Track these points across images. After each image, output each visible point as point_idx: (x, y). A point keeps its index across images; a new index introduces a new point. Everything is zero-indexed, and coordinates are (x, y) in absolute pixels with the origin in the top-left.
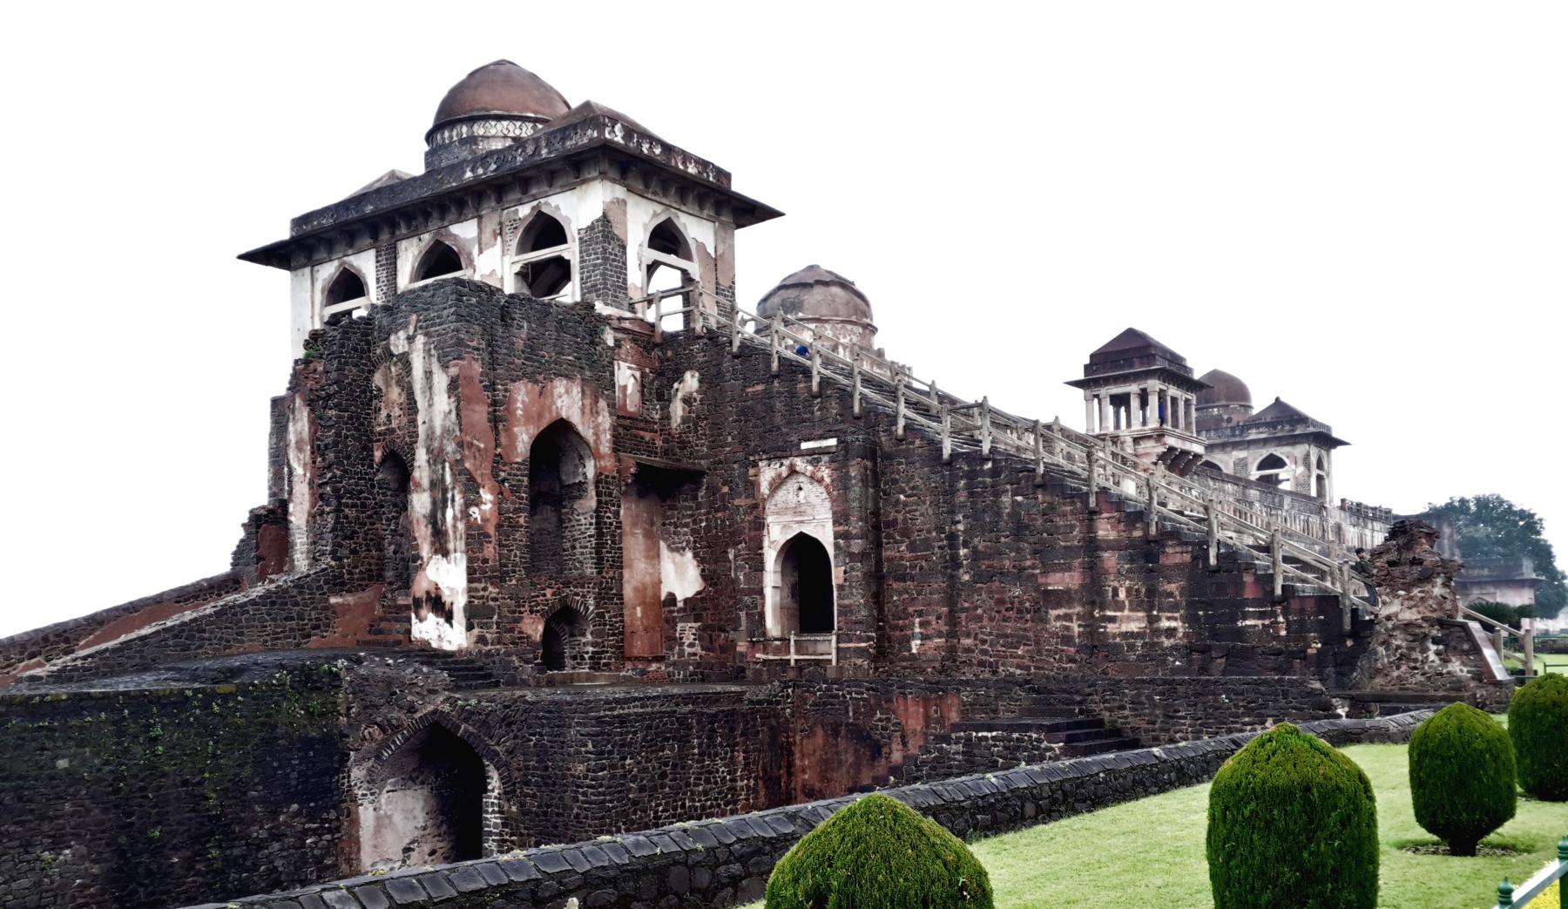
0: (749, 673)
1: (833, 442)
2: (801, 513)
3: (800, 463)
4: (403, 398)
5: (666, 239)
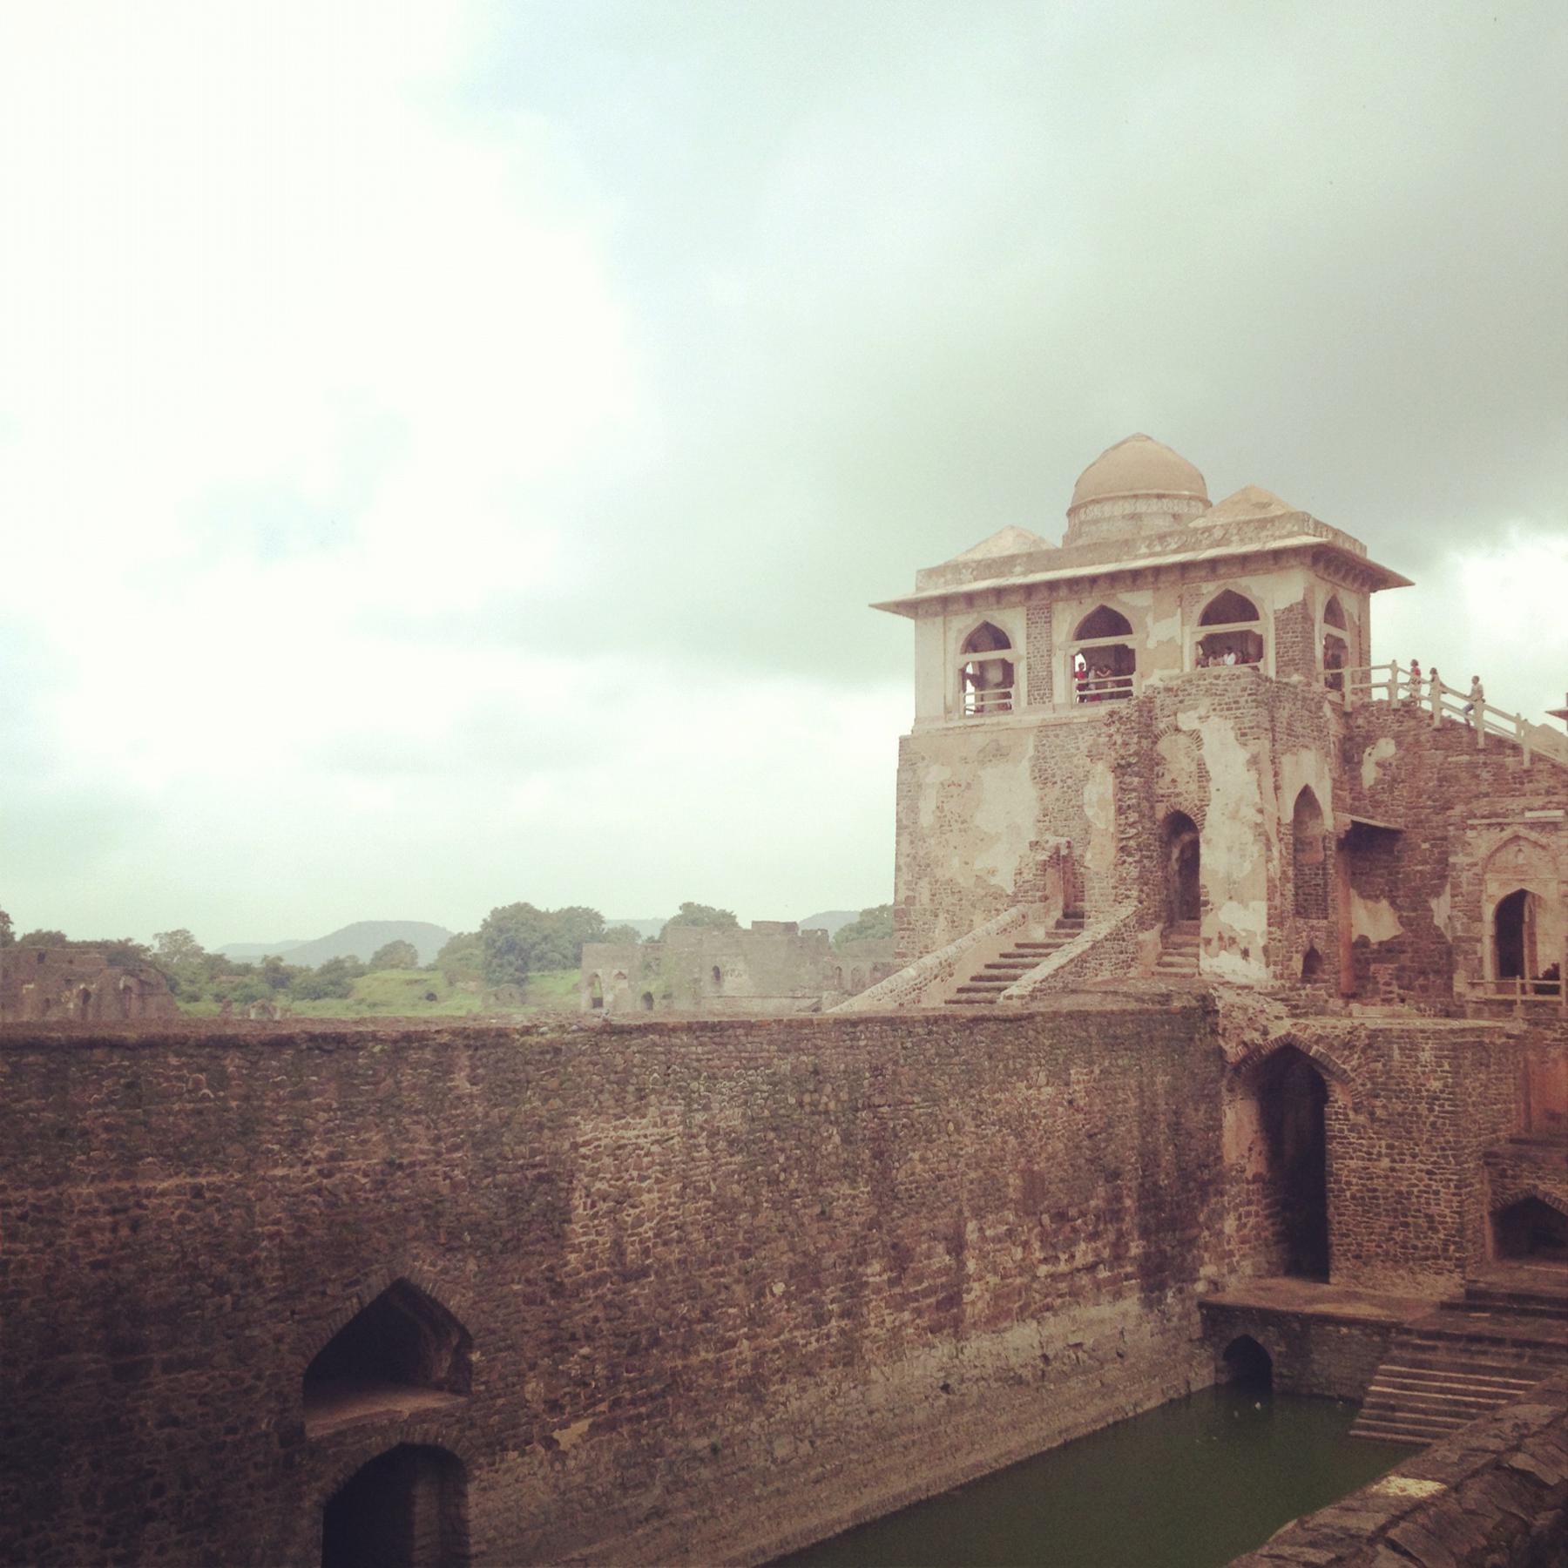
0: (1469, 1009)
1: (1560, 813)
2: (1523, 873)
3: (1523, 832)
4: (1193, 767)
5: (1333, 613)
